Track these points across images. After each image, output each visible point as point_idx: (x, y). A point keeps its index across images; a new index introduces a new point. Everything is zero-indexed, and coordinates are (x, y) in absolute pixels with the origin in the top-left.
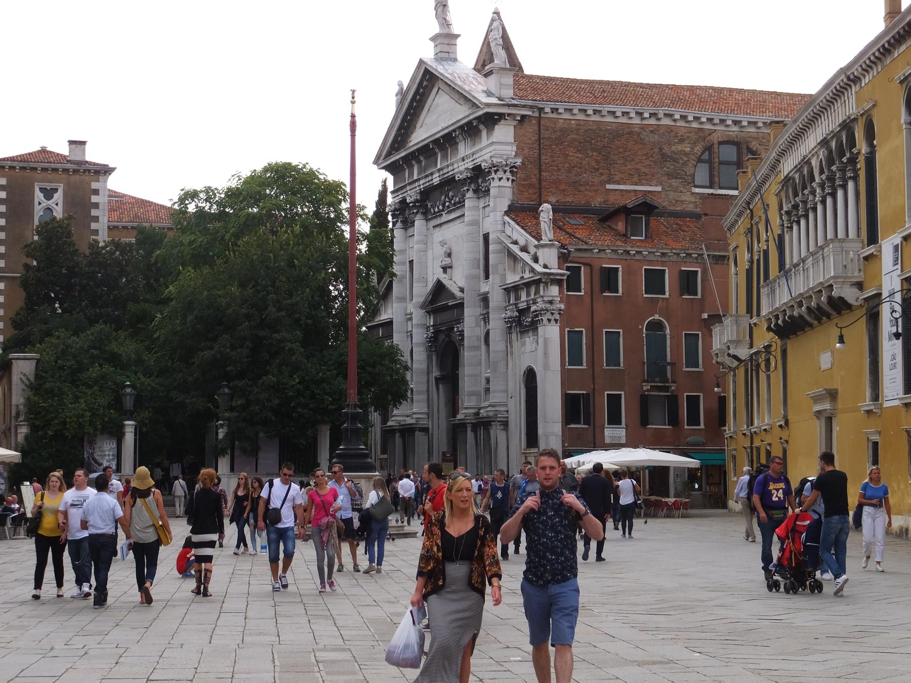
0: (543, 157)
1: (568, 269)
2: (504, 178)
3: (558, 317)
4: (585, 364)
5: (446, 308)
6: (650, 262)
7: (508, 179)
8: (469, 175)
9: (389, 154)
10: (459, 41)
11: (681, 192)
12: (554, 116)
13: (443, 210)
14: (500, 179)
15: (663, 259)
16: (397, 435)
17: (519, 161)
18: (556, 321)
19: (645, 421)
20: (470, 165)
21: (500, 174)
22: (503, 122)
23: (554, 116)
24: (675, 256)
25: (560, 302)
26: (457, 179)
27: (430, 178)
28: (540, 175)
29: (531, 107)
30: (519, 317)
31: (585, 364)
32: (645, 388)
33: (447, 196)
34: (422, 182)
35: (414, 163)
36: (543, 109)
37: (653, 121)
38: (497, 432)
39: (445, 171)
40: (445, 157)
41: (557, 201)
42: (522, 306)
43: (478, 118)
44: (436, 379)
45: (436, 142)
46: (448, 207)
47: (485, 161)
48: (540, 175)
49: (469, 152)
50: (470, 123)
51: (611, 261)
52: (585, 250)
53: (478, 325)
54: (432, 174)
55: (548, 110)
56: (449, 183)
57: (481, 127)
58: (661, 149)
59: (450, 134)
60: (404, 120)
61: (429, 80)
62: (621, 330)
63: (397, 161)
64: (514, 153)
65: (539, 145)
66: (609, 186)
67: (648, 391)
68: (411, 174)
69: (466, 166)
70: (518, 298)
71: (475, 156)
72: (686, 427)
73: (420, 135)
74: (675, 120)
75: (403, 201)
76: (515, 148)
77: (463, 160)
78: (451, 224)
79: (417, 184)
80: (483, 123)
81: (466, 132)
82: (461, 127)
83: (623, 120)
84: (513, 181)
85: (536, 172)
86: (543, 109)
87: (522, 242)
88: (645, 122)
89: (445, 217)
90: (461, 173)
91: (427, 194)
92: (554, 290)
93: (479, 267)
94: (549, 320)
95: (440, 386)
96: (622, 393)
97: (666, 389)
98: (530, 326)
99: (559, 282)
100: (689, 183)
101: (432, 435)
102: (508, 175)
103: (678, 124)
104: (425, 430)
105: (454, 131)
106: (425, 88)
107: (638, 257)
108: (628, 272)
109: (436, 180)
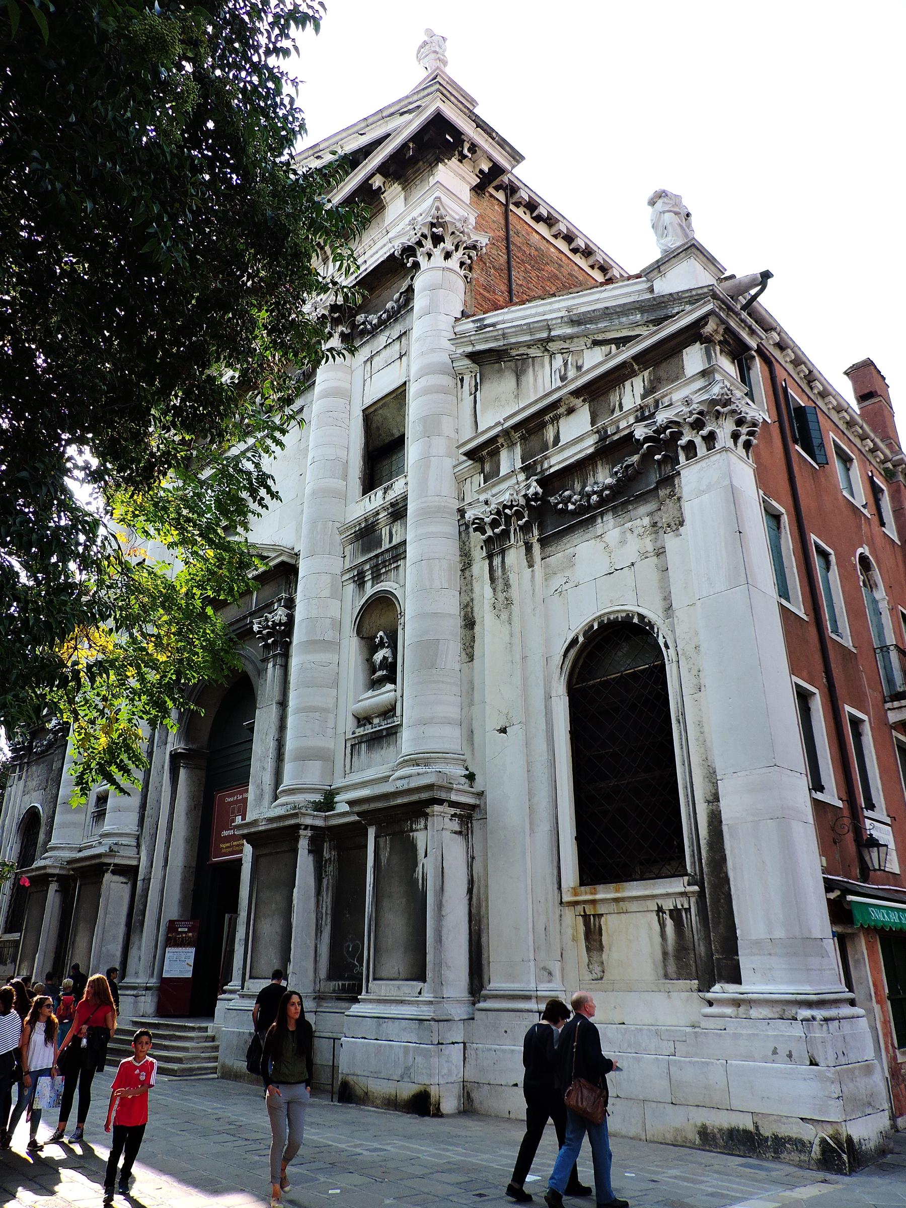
7: (462, 264)
12: (527, 218)
14: (448, 255)
16: (53, 887)
21: (448, 245)
38: (438, 844)
44: (175, 758)
53: (336, 594)
85: (504, 288)
93: (345, 477)
95: (183, 773)
101: (147, 880)
104: (129, 872)
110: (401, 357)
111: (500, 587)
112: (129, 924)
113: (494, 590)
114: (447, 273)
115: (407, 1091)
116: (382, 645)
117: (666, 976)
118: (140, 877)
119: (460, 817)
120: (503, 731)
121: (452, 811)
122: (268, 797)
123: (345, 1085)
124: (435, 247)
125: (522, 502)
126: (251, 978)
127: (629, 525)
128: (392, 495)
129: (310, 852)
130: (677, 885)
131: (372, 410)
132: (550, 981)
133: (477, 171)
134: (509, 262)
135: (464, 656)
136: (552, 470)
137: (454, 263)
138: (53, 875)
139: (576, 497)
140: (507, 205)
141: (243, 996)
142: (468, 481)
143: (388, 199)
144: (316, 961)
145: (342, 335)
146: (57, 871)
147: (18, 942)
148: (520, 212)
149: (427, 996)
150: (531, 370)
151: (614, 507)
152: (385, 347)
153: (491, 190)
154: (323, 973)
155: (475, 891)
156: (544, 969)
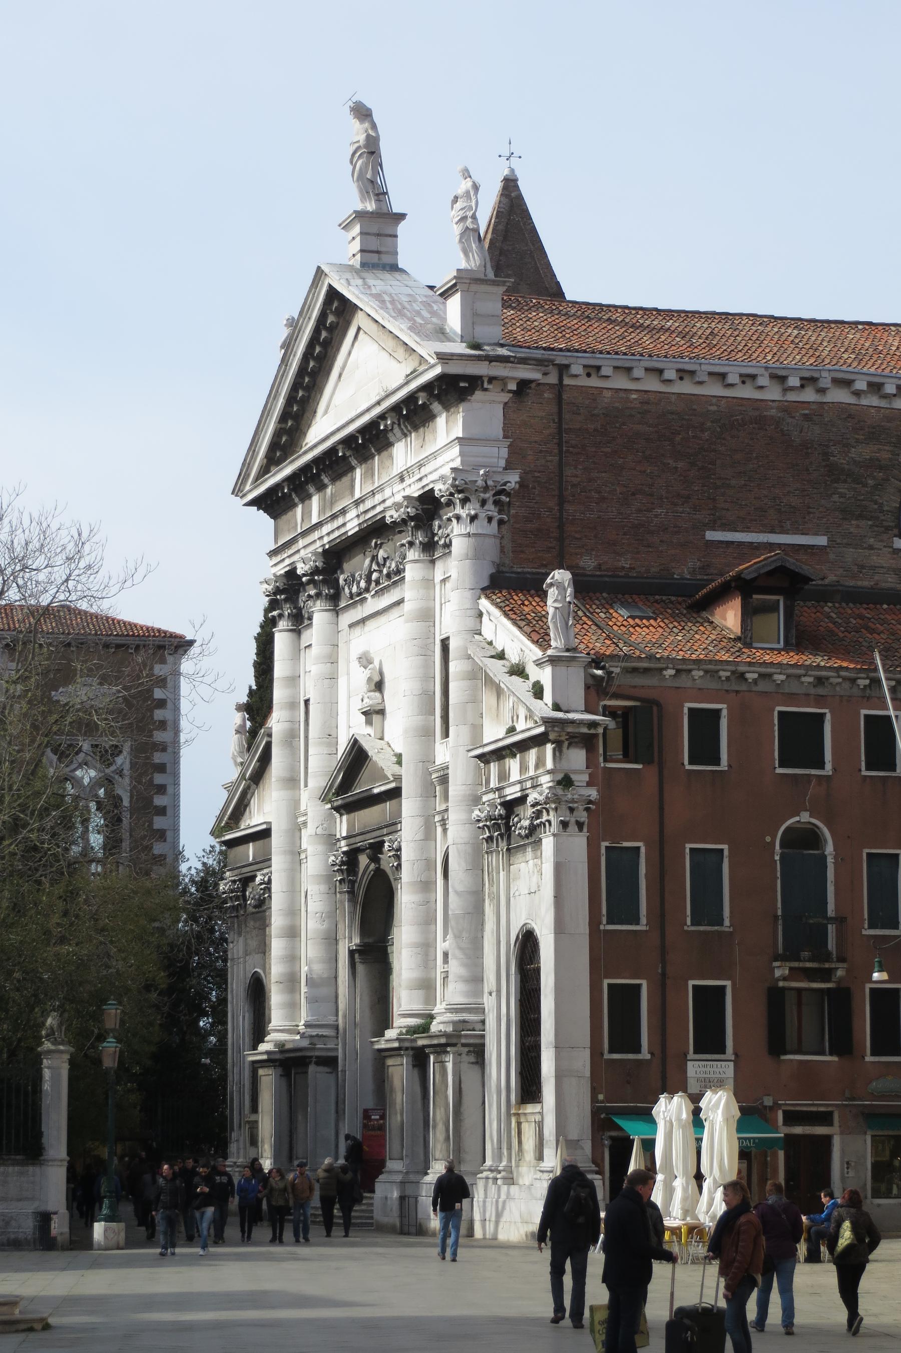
0: (568, 472)
1: (609, 712)
2: (482, 516)
3: (583, 816)
4: (644, 920)
5: (370, 800)
6: (791, 698)
7: (490, 519)
8: (411, 511)
9: (265, 471)
10: (402, 229)
11: (871, 548)
12: (594, 382)
13: (367, 590)
15: (821, 691)
17: (513, 479)
18: (580, 825)
19: (777, 1045)
20: (415, 491)
22: (478, 395)
23: (594, 382)
24: (847, 685)
25: (589, 784)
26: (388, 520)
27: (340, 521)
28: (561, 510)
29: (540, 363)
30: (507, 817)
31: (644, 920)
32: (778, 973)
33: (374, 558)
34: (326, 529)
35: (312, 489)
36: (567, 367)
37: (809, 395)
39: (369, 504)
40: (369, 475)
41: (599, 567)
42: (512, 792)
43: (427, 387)
44: (352, 953)
45: (348, 441)
46: (377, 582)
47: (442, 478)
48: (561, 510)
49: (412, 460)
50: (411, 399)
51: (702, 694)
52: (646, 670)
54: (343, 512)
55: (577, 369)
56: (377, 530)
57: (436, 407)
58: (826, 455)
59: (372, 425)
60: (291, 399)
61: (339, 313)
62: (725, 847)
63: (277, 487)
64: (502, 463)
65: (560, 445)
66: (711, 535)
67: (785, 979)
68: (307, 514)
69: (407, 492)
70: (503, 776)
71: (424, 471)
72: (869, 1058)
73: (326, 427)
74: (857, 394)
75: (291, 574)
76: (504, 452)
77: (402, 479)
78: (382, 619)
79: (316, 535)
80: (438, 398)
81: (407, 418)
82: (396, 408)
83: (746, 392)
84: (501, 522)
86: (567, 367)
87: (513, 657)
88: (792, 397)
89: (372, 604)
90: (397, 506)
91: (335, 556)
92: (577, 758)
94: (564, 825)
95: (360, 968)
96: (728, 983)
97: (826, 975)
98: (527, 836)
99: (586, 740)
100: (888, 529)
101: (344, 1071)
102: (490, 506)
103: (865, 402)
105: (382, 417)
106: (331, 329)
107: (762, 686)
108: (739, 719)
109: (352, 524)
112: (337, 1112)
118: (340, 1069)
119: (474, 1052)
129: (414, 1066)
134: (560, 465)
136: (508, 798)
139: (519, 825)
151: (531, 843)
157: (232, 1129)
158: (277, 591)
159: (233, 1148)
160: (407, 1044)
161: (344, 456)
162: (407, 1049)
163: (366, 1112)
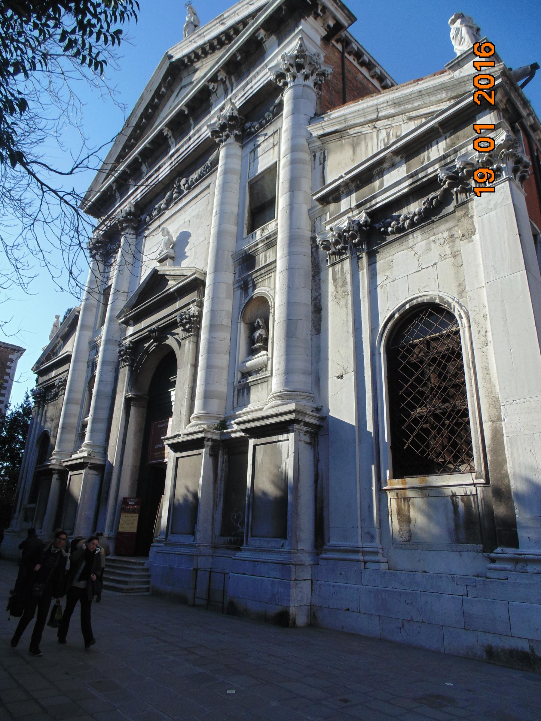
7: (315, 84)
12: (355, 63)
14: (306, 77)
44: (128, 401)
79: (132, 197)
95: (133, 410)
110: (274, 146)
111: (340, 284)
113: (336, 286)
114: (306, 88)
115: (273, 610)
116: (259, 327)
117: (458, 541)
118: (106, 472)
120: (341, 377)
121: (305, 429)
122: (184, 422)
123: (232, 604)
124: (298, 72)
125: (356, 228)
126: (172, 533)
127: (433, 238)
128: (266, 233)
129: (210, 455)
130: (468, 478)
131: (254, 182)
132: (372, 542)
133: (326, 25)
135: (314, 330)
137: (310, 82)
138: (55, 470)
140: (343, 54)
141: (166, 544)
142: (318, 219)
143: (267, 46)
144: (213, 524)
145: (236, 136)
146: (57, 467)
147: (34, 509)
148: (351, 58)
149: (286, 549)
150: (363, 143)
152: (264, 141)
153: (333, 42)
154: (217, 532)
155: (319, 481)
156: (368, 533)
157: (15, 512)
158: (98, 242)
159: (14, 522)
160: (210, 436)
161: (167, 135)
162: (208, 439)
163: (125, 499)
